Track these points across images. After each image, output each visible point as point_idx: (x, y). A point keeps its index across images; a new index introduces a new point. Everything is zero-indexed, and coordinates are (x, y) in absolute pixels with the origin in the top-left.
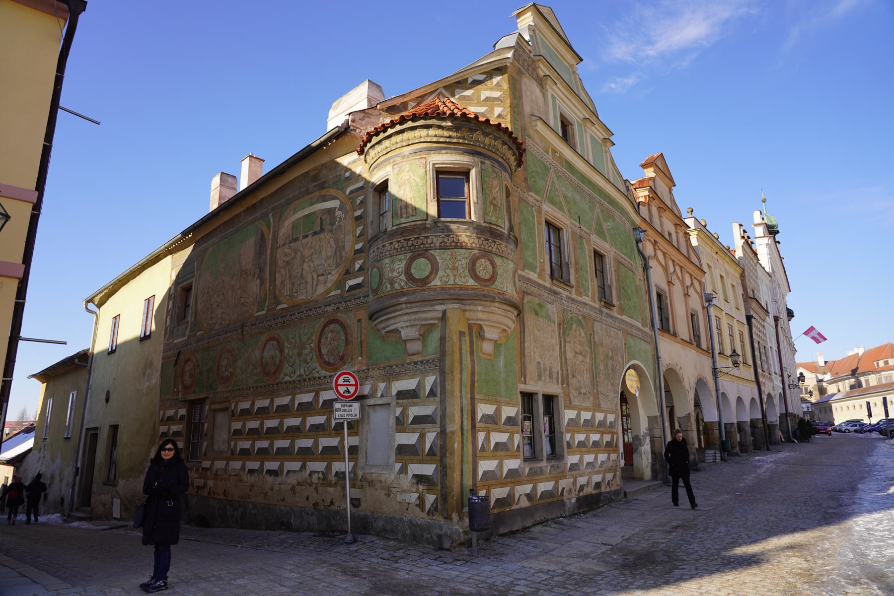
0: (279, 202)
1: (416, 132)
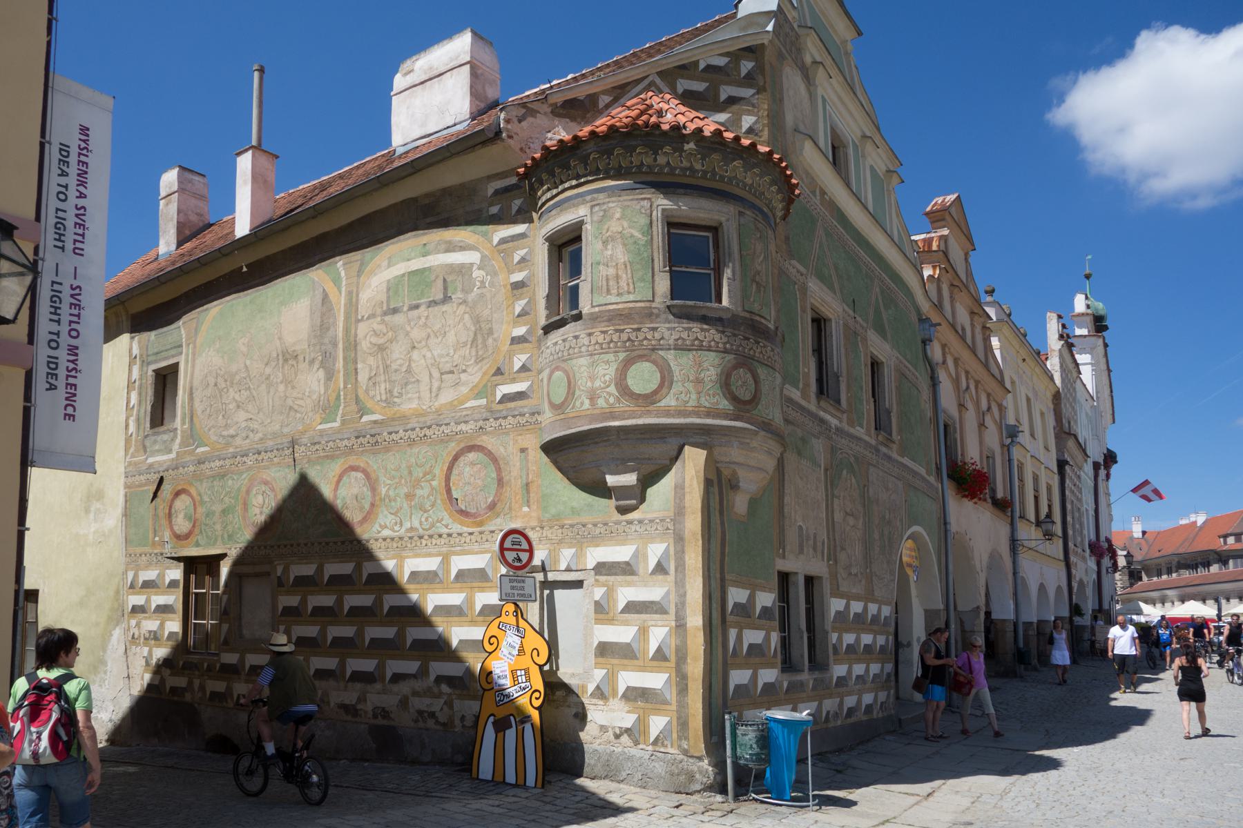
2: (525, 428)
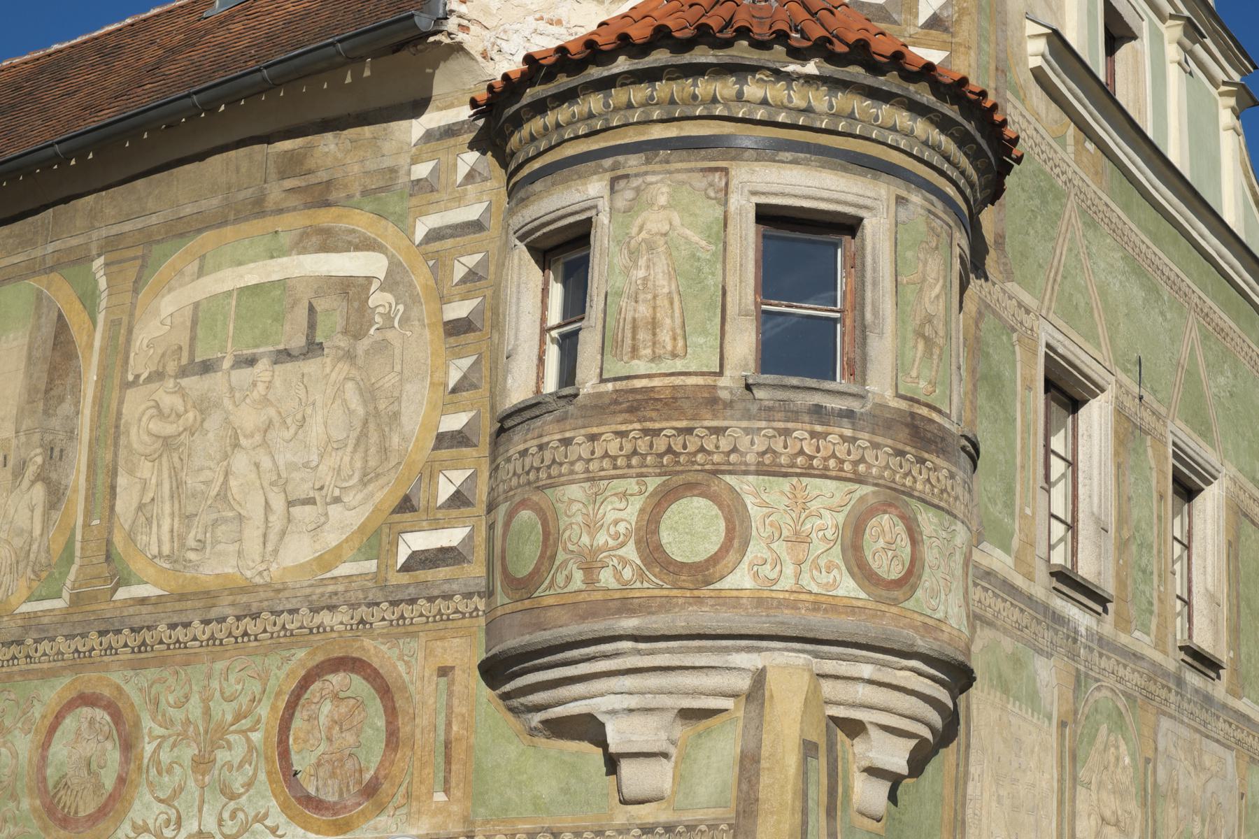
0: (139, 224)
1: (700, 81)
2: (450, 624)
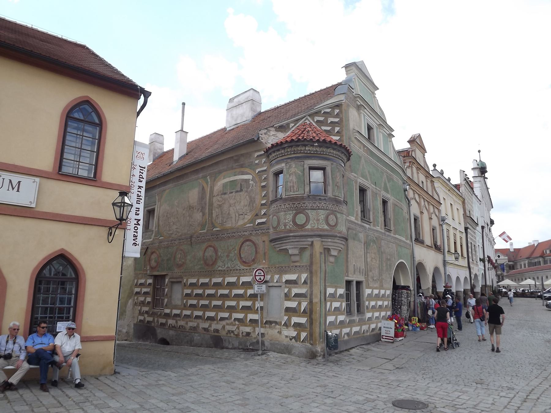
0: (214, 171)
